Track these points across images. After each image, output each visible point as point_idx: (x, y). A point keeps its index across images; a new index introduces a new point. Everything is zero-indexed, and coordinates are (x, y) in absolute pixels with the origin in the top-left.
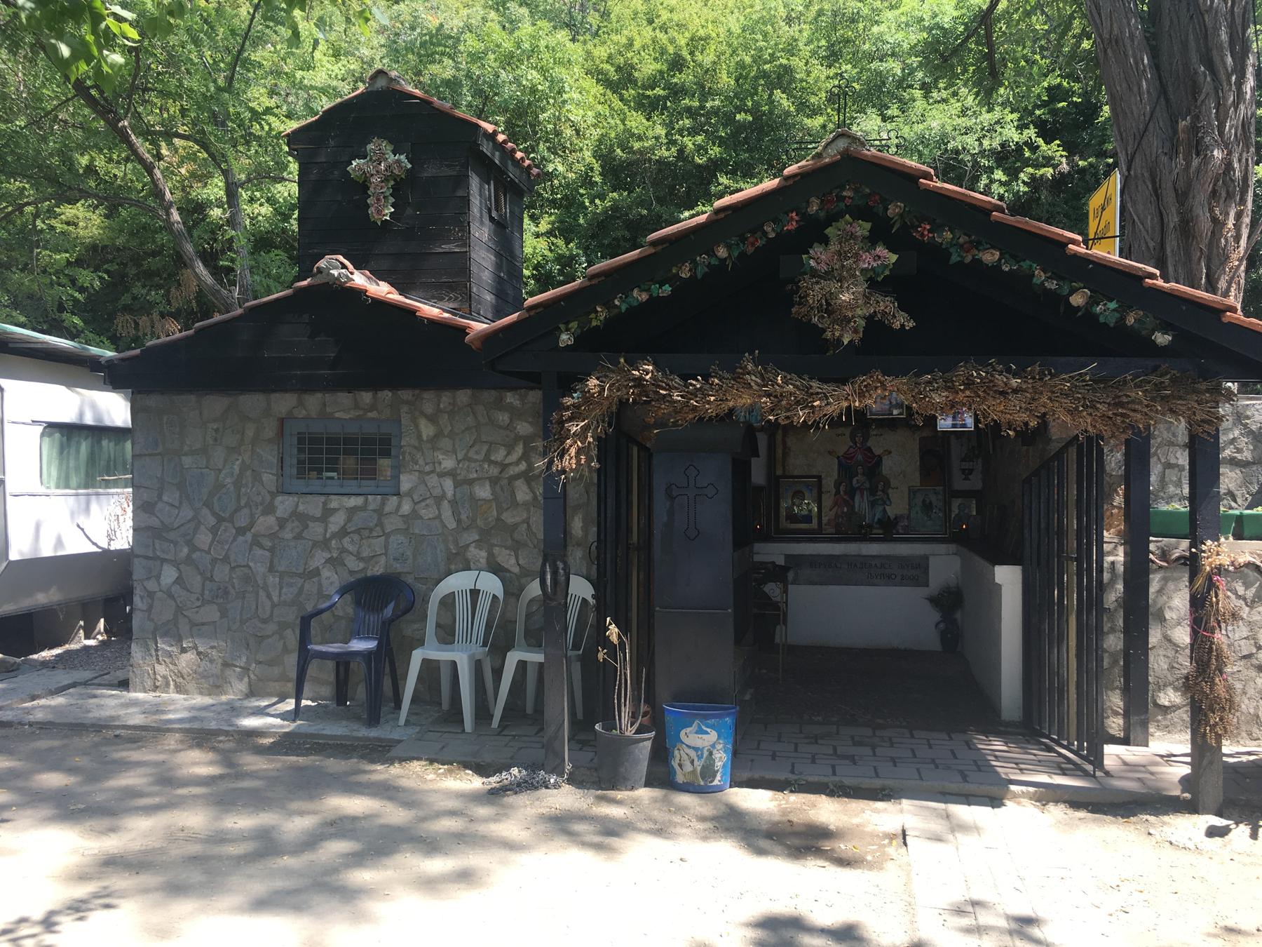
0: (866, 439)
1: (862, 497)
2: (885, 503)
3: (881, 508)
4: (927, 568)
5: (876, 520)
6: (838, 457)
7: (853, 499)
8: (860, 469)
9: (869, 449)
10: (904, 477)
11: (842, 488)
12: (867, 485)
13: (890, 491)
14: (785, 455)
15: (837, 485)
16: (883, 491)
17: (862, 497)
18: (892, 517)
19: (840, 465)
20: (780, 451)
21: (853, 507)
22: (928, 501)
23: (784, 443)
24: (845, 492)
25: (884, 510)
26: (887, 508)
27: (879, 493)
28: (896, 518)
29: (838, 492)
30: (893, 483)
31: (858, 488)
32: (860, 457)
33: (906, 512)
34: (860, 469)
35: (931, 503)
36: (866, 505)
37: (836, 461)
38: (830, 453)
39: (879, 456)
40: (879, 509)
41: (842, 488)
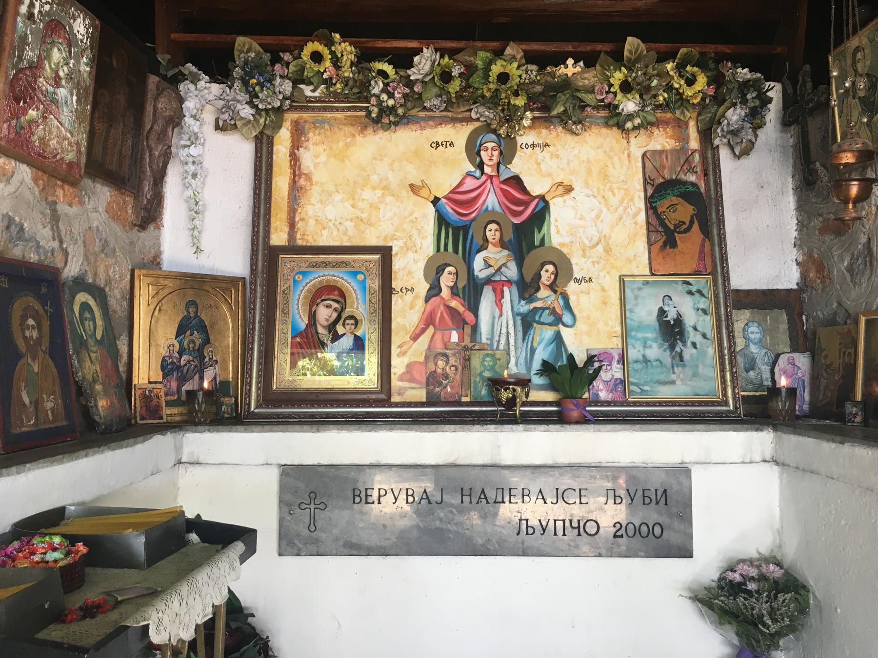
0: (507, 152)
1: (499, 303)
2: (558, 320)
3: (548, 333)
4: (687, 505)
5: (537, 365)
6: (436, 201)
7: (474, 308)
8: (492, 232)
9: (516, 181)
10: (608, 250)
11: (446, 280)
12: (512, 271)
13: (572, 288)
14: (295, 191)
15: (434, 271)
16: (552, 287)
17: (499, 303)
18: (580, 359)
19: (442, 221)
20: (281, 183)
21: (475, 328)
22: (671, 316)
23: (294, 159)
24: (454, 291)
25: (558, 339)
26: (565, 332)
27: (544, 293)
28: (590, 359)
29: (435, 289)
30: (580, 266)
31: (488, 281)
32: (491, 201)
33: (614, 344)
34: (492, 232)
35: (679, 321)
36: (508, 323)
37: (431, 210)
38: (414, 189)
39: (542, 198)
40: (543, 334)
41: (446, 280)
